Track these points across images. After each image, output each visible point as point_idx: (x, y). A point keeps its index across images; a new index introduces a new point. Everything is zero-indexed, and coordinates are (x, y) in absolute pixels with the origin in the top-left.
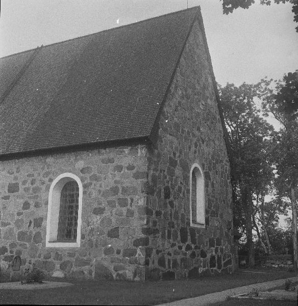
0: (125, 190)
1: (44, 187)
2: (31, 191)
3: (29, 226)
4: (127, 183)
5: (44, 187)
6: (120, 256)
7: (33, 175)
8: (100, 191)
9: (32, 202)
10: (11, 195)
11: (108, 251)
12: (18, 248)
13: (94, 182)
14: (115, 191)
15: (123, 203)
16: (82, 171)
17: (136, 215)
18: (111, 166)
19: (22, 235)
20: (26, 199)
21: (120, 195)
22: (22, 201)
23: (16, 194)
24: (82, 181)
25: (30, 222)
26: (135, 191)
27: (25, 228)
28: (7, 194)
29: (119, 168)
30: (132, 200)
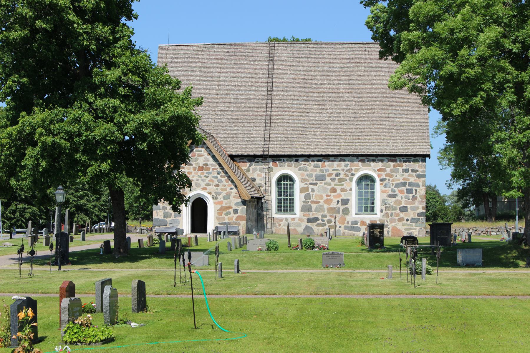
0: (410, 184)
1: (348, 178)
2: (336, 181)
3: (337, 204)
4: (412, 180)
5: (348, 178)
6: (409, 222)
7: (338, 170)
8: (393, 184)
9: (338, 188)
10: (319, 182)
11: (401, 220)
12: (329, 218)
13: (388, 178)
14: (404, 184)
15: (409, 191)
16: (379, 170)
17: (419, 199)
18: (401, 169)
19: (331, 210)
20: (333, 186)
21: (407, 187)
22: (329, 187)
23: (323, 182)
24: (379, 176)
25: (338, 202)
26: (418, 186)
27: (334, 205)
28: (315, 182)
29: (406, 171)
30: (416, 190)
